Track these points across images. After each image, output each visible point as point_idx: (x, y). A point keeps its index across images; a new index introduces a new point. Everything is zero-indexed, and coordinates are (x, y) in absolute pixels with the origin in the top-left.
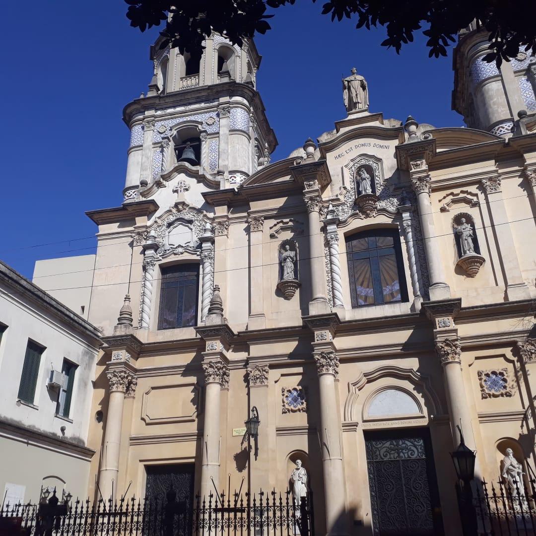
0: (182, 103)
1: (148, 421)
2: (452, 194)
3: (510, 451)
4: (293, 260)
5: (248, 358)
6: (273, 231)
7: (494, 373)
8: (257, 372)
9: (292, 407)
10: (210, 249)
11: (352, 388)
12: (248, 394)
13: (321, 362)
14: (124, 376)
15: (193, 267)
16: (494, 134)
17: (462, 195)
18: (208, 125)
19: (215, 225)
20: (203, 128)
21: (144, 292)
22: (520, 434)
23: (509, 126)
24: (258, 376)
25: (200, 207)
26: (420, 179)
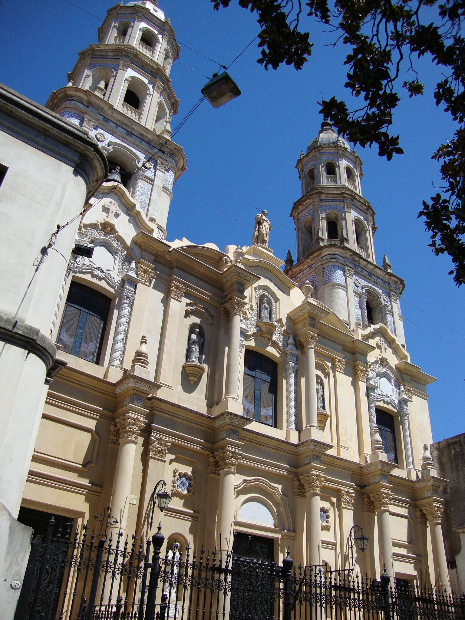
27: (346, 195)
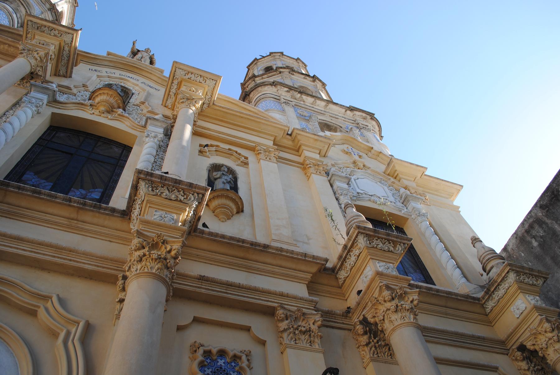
2: (217, 146)
7: (222, 353)
27: (281, 70)
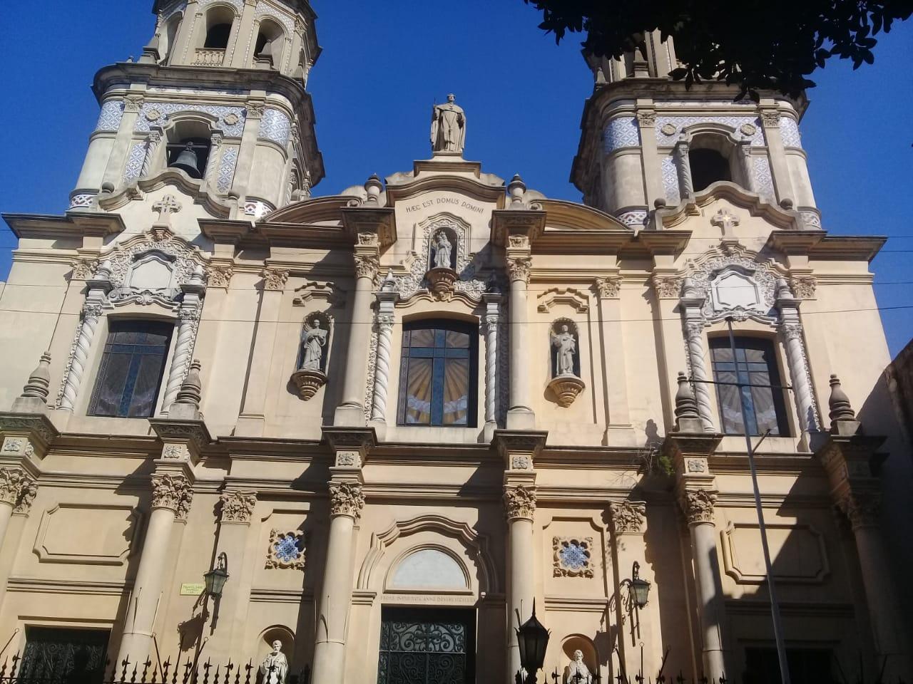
0: (189, 84)
1: (44, 555)
2: (556, 290)
3: (579, 653)
4: (322, 343)
5: (225, 479)
6: (298, 295)
7: (574, 542)
8: (237, 502)
9: (282, 561)
10: (195, 305)
11: (377, 541)
12: (217, 534)
13: (339, 497)
14: (18, 479)
15: (163, 327)
16: (621, 221)
17: (568, 294)
18: (227, 124)
19: (210, 269)
20: (217, 127)
21: (75, 354)
22: (598, 632)
23: (641, 216)
24: (237, 508)
25: (191, 240)
26: (518, 262)
